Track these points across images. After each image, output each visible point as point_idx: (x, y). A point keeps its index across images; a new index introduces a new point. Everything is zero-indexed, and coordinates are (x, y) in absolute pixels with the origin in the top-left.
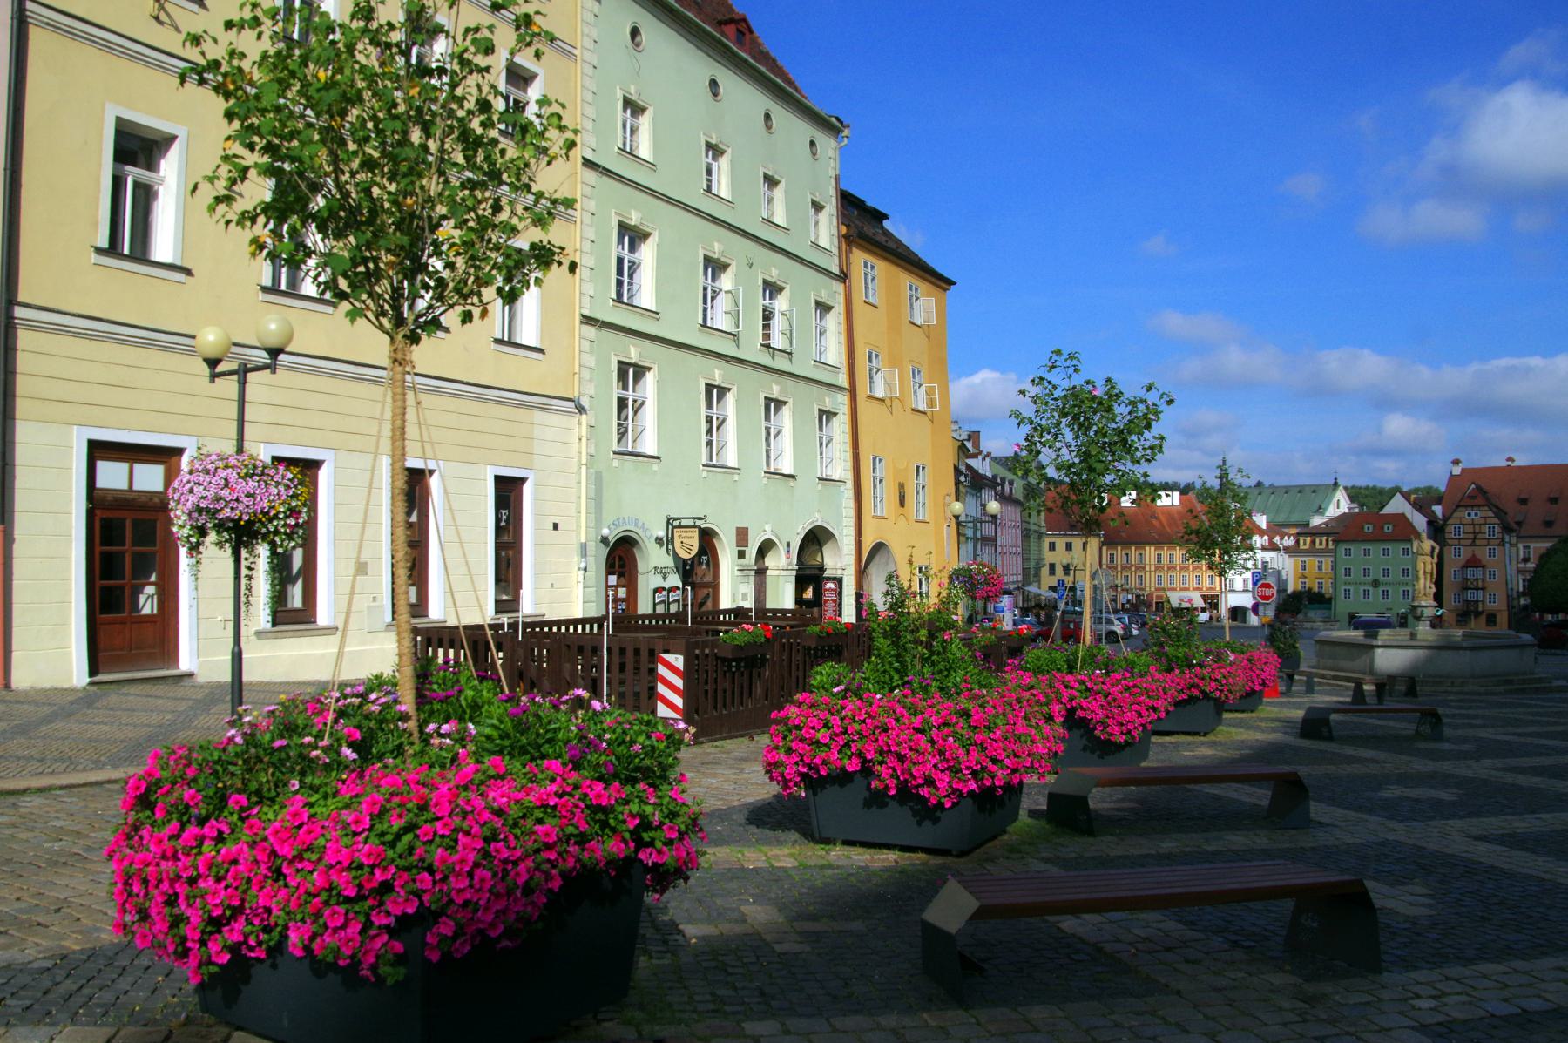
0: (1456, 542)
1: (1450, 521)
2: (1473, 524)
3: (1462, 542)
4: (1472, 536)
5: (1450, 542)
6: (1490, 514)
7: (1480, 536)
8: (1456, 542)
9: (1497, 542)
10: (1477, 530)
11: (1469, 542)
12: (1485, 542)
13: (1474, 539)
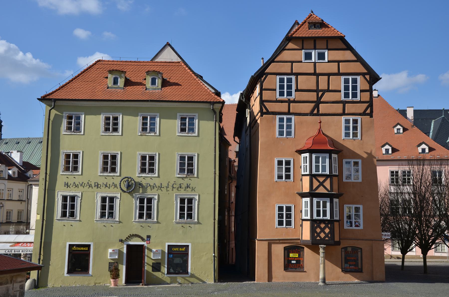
0: (283, 107)
1: (272, 68)
2: (315, 74)
3: (294, 107)
4: (313, 96)
5: (271, 107)
6: (348, 55)
7: (327, 97)
8: (283, 107)
9: (361, 108)
10: (323, 85)
11: (308, 107)
12: (338, 108)
13: (318, 102)
